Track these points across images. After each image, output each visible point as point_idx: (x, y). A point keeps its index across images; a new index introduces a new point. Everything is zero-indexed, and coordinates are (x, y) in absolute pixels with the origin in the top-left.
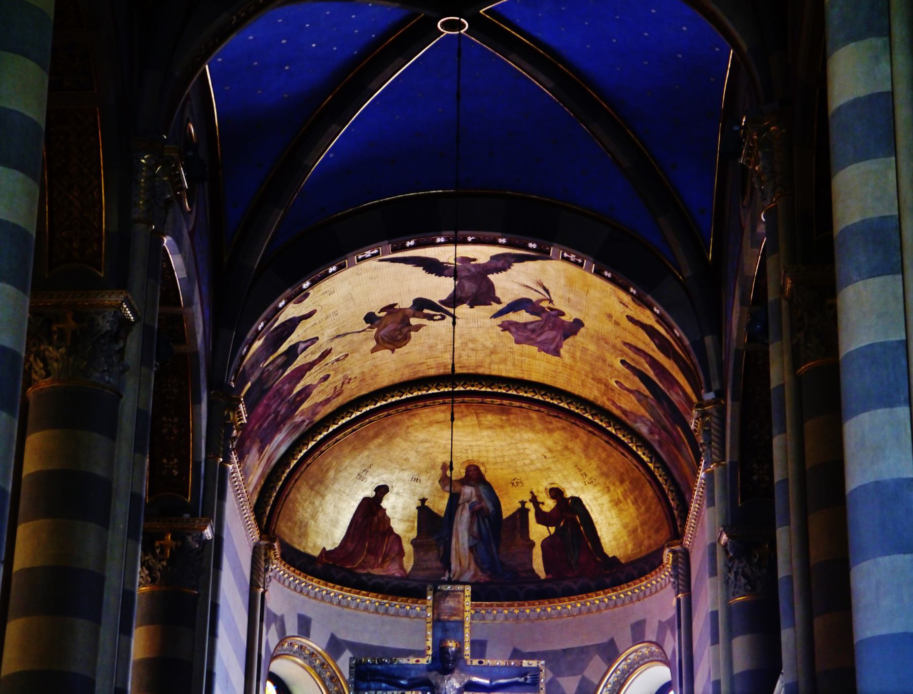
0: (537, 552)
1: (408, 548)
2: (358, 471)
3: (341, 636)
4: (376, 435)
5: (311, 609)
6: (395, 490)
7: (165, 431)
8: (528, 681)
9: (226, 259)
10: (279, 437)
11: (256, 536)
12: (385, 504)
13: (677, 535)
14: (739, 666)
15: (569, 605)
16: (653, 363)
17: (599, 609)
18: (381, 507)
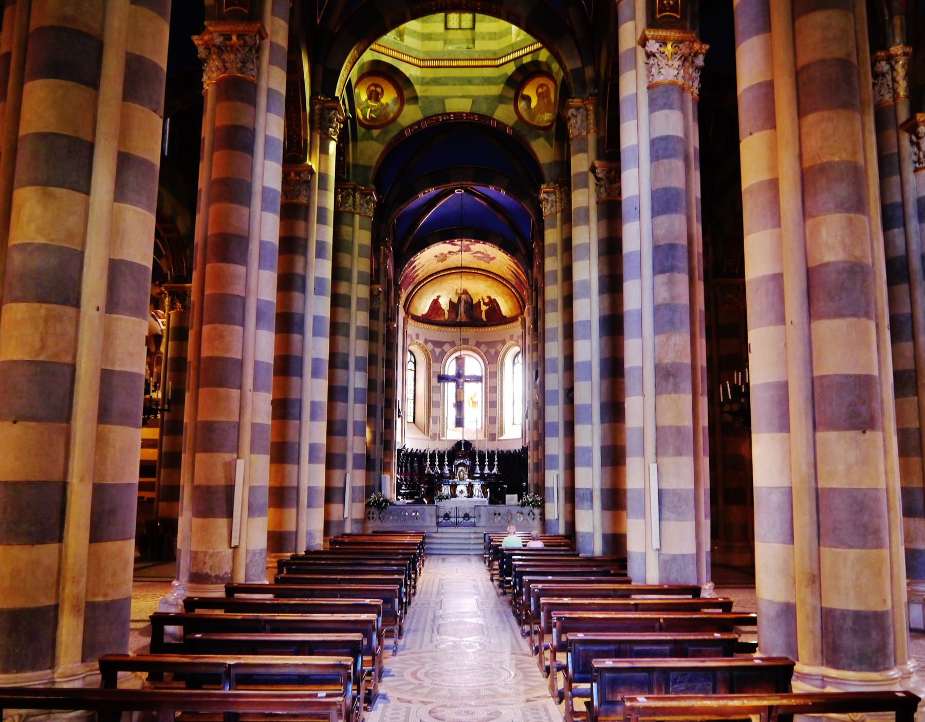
0: (483, 314)
1: (446, 312)
3: (428, 338)
5: (419, 331)
10: (410, 287)
12: (439, 300)
13: (522, 313)
14: (534, 360)
15: (492, 329)
16: (516, 270)
17: (501, 330)
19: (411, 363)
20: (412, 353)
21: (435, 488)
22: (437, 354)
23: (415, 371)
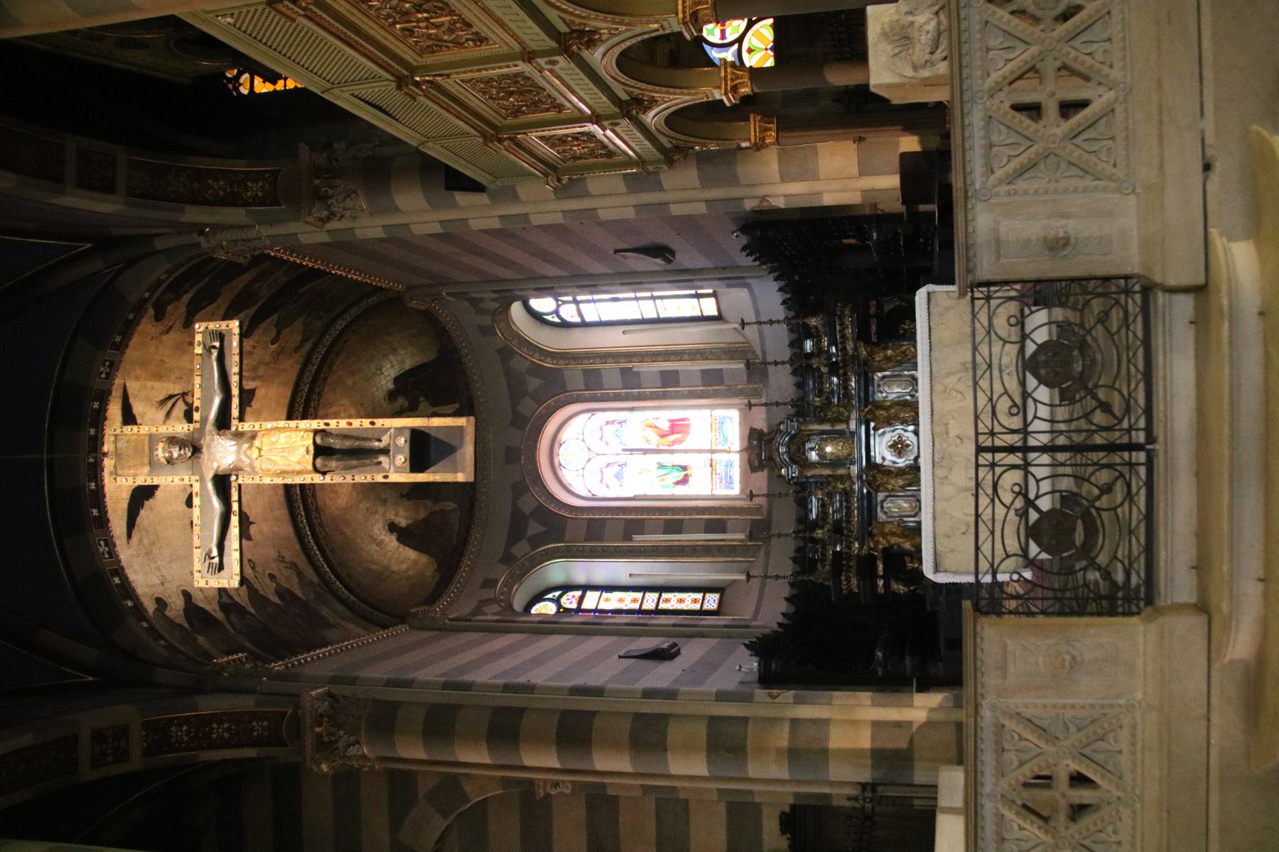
2: (374, 546)
4: (342, 533)
6: (392, 517)
7: (226, 735)
8: (217, 344)
9: (91, 679)
11: (403, 628)
18: (406, 529)
19: (563, 600)
20: (538, 598)
21: (884, 549)
22: (543, 529)
23: (586, 588)
